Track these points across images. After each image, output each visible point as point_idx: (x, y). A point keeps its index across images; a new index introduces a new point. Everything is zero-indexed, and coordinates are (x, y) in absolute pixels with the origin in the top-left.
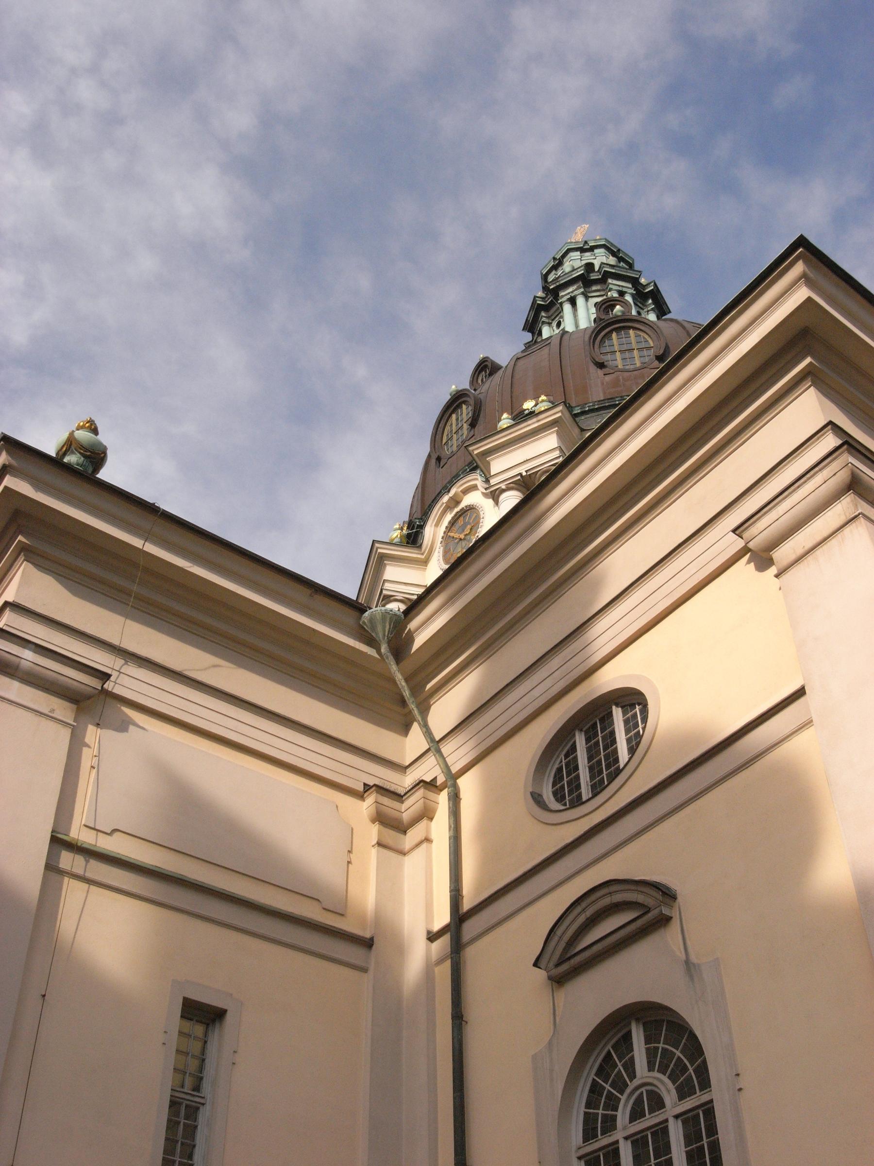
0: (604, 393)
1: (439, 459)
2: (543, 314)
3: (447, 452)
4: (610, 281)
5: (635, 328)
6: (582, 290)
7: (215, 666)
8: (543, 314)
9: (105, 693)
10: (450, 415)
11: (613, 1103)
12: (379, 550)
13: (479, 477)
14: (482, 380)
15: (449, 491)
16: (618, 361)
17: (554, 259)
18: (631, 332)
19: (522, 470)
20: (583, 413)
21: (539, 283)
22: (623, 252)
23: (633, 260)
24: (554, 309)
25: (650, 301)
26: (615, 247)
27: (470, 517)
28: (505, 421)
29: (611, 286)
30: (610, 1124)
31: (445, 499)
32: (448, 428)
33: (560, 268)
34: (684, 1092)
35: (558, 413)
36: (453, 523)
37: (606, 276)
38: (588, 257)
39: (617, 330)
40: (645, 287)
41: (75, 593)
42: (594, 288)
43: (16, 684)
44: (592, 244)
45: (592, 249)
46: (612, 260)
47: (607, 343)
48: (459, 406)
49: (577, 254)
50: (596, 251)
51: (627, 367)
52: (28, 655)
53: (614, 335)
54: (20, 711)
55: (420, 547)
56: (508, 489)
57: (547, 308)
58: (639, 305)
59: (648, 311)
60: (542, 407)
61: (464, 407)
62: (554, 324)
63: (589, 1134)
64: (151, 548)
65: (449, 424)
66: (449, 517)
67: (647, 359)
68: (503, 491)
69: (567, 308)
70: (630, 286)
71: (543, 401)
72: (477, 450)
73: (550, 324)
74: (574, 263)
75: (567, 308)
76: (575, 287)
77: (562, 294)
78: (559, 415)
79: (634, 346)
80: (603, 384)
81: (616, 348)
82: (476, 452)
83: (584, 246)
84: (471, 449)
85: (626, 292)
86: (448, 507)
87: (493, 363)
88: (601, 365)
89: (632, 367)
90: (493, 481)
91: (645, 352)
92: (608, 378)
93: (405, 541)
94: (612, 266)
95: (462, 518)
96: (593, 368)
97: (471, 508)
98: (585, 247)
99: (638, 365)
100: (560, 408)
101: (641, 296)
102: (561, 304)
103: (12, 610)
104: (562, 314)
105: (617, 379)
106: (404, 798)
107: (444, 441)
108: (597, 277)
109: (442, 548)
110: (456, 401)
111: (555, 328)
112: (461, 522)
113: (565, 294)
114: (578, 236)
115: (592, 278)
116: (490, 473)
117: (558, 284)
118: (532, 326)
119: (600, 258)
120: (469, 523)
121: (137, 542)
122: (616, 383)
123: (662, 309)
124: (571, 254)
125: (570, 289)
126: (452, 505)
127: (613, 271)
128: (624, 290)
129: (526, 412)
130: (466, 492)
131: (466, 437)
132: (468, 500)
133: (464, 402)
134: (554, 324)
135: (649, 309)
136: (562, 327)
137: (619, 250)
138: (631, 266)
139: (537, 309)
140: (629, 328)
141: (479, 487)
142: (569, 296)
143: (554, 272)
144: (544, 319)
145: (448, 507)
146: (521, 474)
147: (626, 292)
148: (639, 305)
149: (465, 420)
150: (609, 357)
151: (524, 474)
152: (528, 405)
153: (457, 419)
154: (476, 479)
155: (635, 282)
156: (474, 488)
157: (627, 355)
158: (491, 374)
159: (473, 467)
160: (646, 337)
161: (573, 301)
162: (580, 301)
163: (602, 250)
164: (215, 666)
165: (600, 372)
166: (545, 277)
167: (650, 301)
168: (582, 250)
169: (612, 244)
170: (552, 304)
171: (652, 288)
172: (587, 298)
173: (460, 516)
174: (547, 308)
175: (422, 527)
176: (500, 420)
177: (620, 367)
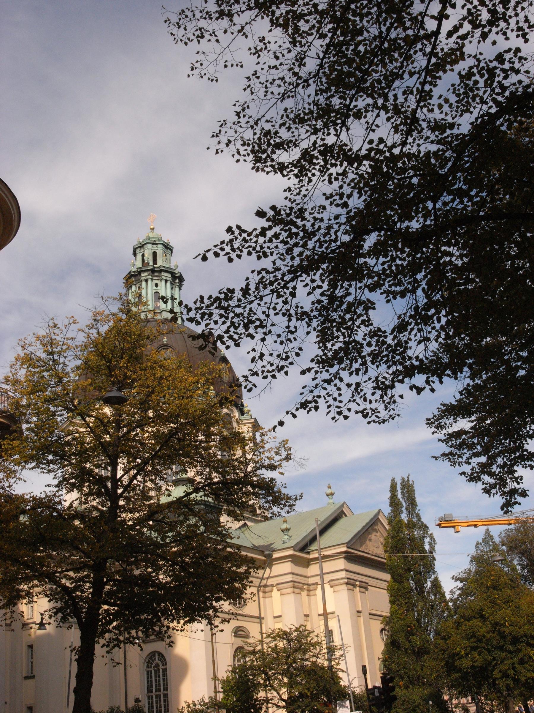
11: (152, 664)
25: (177, 281)
30: (151, 667)
34: (163, 665)
38: (155, 247)
42: (156, 274)
45: (157, 244)
49: (150, 245)
57: (135, 276)
63: (147, 667)
69: (144, 283)
75: (144, 283)
77: (143, 275)
125: (146, 274)
128: (168, 279)
161: (146, 281)
162: (149, 282)
168: (153, 244)
172: (152, 279)
174: (135, 276)
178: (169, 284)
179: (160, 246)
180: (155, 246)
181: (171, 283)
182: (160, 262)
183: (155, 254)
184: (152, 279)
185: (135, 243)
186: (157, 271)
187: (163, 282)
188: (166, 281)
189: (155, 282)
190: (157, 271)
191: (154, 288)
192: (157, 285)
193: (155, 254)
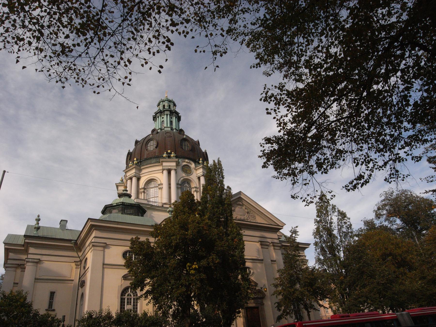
38: (164, 103)
42: (163, 113)
45: (165, 101)
50: (166, 102)
69: (157, 119)
88: (147, 150)
122: (148, 154)
161: (158, 117)
162: (160, 117)
168: (163, 102)
172: (161, 116)
178: (168, 116)
179: (172, 103)
181: (170, 115)
182: (166, 107)
183: (164, 106)
184: (161, 116)
185: (157, 104)
186: (163, 112)
187: (166, 116)
188: (167, 115)
189: (162, 117)
191: (162, 119)
192: (163, 118)
193: (164, 106)
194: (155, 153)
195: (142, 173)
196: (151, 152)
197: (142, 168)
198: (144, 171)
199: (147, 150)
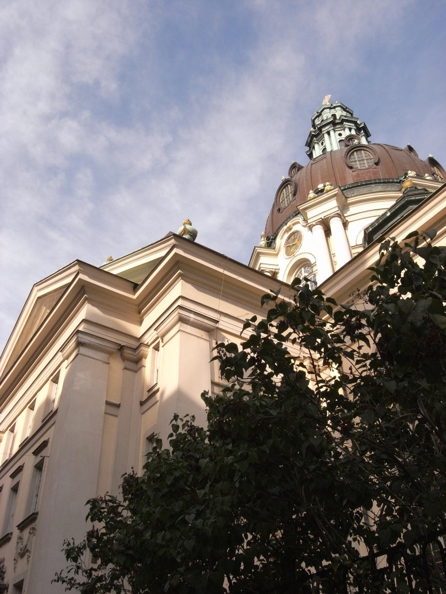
0: (353, 180)
1: (279, 210)
2: (315, 139)
3: (283, 206)
4: (345, 123)
5: (364, 150)
6: (333, 128)
7: (247, 314)
8: (315, 139)
9: (218, 328)
10: (283, 189)
12: (257, 251)
13: (300, 218)
14: (294, 172)
15: (286, 224)
16: (358, 165)
17: (318, 112)
18: (362, 151)
19: (322, 216)
20: (345, 189)
21: (310, 123)
22: (348, 108)
23: (353, 112)
24: (319, 136)
25: (362, 131)
26: (345, 106)
27: (297, 235)
28: (312, 194)
29: (345, 126)
31: (285, 228)
32: (282, 195)
33: (320, 117)
35: (336, 191)
36: (289, 238)
37: (343, 121)
39: (356, 151)
40: (359, 125)
41: (198, 290)
42: (338, 126)
43: (189, 327)
44: (334, 105)
45: (334, 108)
46: (344, 113)
47: (352, 157)
48: (287, 185)
50: (337, 108)
51: (362, 168)
52: (192, 316)
53: (355, 153)
54: (193, 337)
55: (274, 248)
56: (316, 224)
57: (316, 136)
58: (358, 133)
59: (362, 136)
60: (328, 188)
61: (289, 186)
62: (320, 143)
64: (221, 270)
65: (282, 194)
66: (287, 235)
67: (370, 164)
68: (314, 225)
69: (326, 136)
70: (354, 125)
71: (328, 185)
72: (301, 208)
73: (318, 143)
74: (327, 115)
75: (326, 136)
76: (329, 126)
77: (323, 130)
78: (337, 192)
79: (364, 158)
80: (352, 176)
81: (357, 159)
82: (301, 209)
83: (331, 106)
84: (298, 207)
85: (352, 128)
86: (286, 231)
87: (299, 165)
88: (351, 168)
89: (364, 168)
90: (309, 221)
91: (369, 161)
92: (354, 173)
93: (266, 245)
94: (346, 116)
95: (293, 236)
96: (347, 169)
97: (297, 232)
98: (331, 107)
99: (367, 167)
100: (337, 189)
101: (358, 130)
102: (323, 134)
103: (182, 299)
104: (323, 139)
105: (358, 174)
106: (318, 361)
107: (281, 202)
108: (339, 122)
109: (285, 249)
110: (285, 184)
111: (321, 145)
112: (293, 237)
113: (325, 130)
114: (326, 102)
115: (336, 122)
116: (307, 217)
117: (321, 125)
118: (310, 144)
119: (339, 113)
120: (296, 238)
121: (221, 270)
122: (358, 176)
123: (367, 135)
124: (325, 110)
125: (327, 128)
126: (288, 230)
127: (346, 119)
128: (351, 127)
129: (320, 189)
130: (294, 224)
131: (292, 200)
132: (295, 229)
133: (289, 184)
134: (320, 143)
135: (362, 135)
136: (324, 145)
137: (346, 108)
138: (352, 114)
139: (312, 137)
140: (362, 150)
141: (300, 222)
142: (326, 131)
143: (317, 118)
144: (315, 141)
145: (286, 231)
146: (321, 218)
147: (352, 128)
148: (358, 133)
149: (290, 192)
150: (353, 163)
151: (323, 218)
152: (320, 186)
153: (286, 191)
154: (299, 219)
155: (355, 123)
156: (298, 223)
157: (362, 162)
158: (298, 170)
159: (297, 213)
160: (369, 154)
161: (328, 133)
162: (332, 133)
163: (339, 108)
164: (247, 314)
165: (351, 171)
166: (313, 121)
167: (362, 131)
168: (330, 108)
169: (344, 105)
170: (318, 134)
171: (363, 125)
172: (335, 131)
173: (292, 235)
174: (316, 136)
175: (275, 239)
176: (309, 194)
177: (359, 168)
180: (333, 110)
186: (338, 124)
190: (338, 124)
194: (375, 173)
195: (348, 213)
196: (367, 173)
197: (350, 200)
198: (352, 210)
199: (351, 168)
